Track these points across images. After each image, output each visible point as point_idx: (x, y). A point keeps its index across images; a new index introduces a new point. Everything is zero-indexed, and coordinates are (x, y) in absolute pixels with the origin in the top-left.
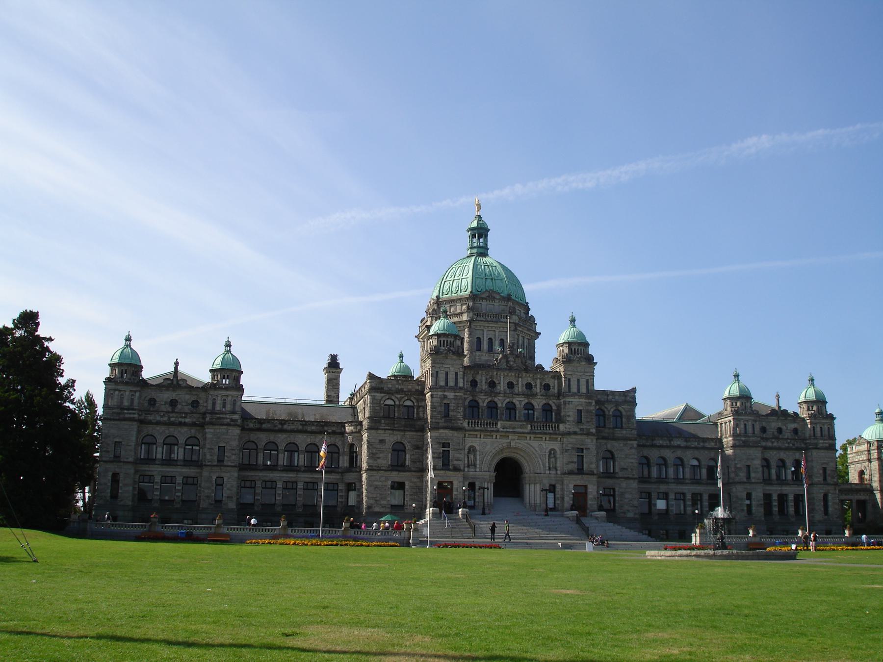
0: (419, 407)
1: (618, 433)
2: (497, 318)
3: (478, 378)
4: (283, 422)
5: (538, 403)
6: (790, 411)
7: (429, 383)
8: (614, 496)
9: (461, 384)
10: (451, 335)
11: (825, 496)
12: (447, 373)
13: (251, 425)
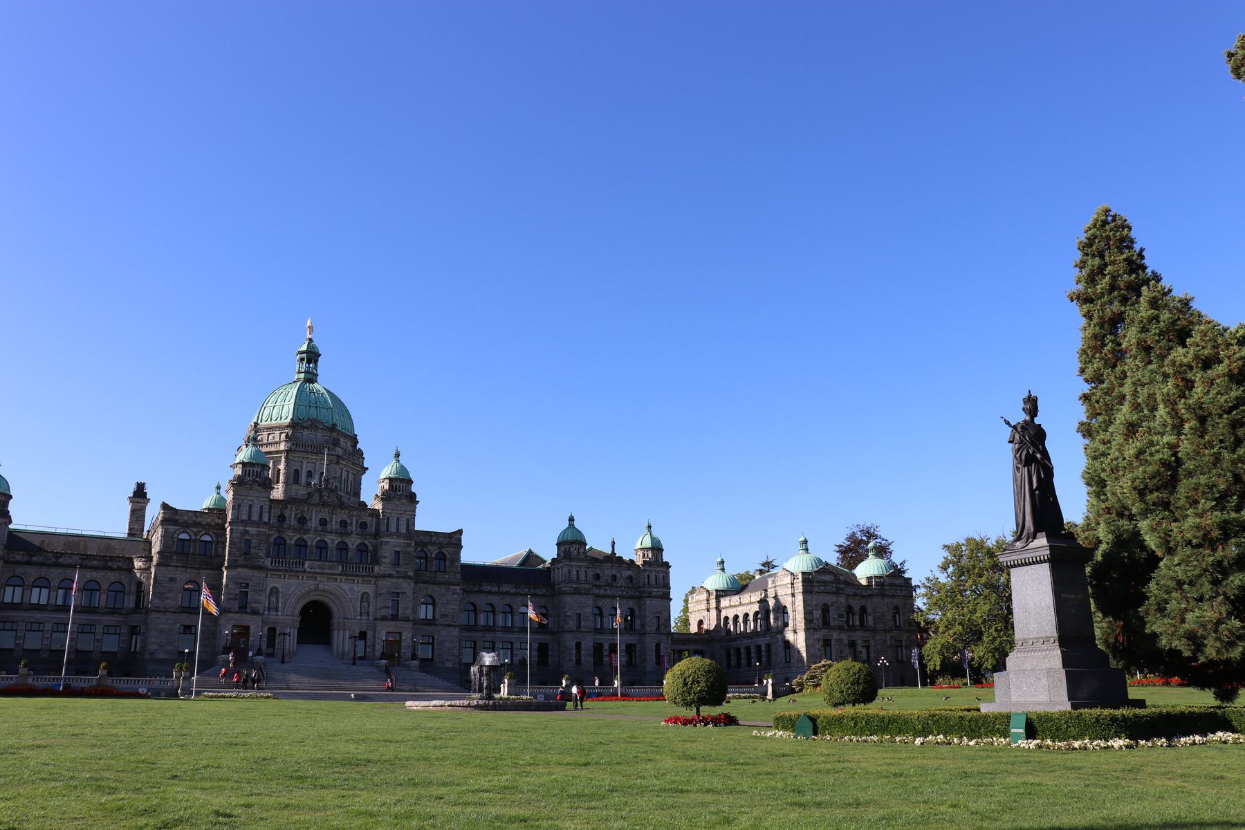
1: (441, 577)
3: (287, 513)
4: (58, 555)
5: (353, 542)
6: (626, 558)
8: (432, 644)
9: (266, 519)
10: (258, 464)
11: (658, 646)
13: (18, 558)
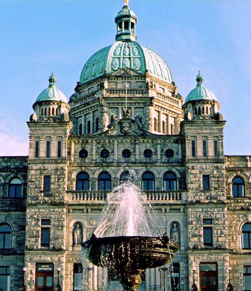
0: (25, 184)
3: (88, 148)
12: (48, 144)
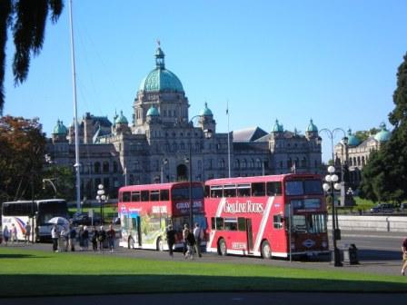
2: (171, 102)
5: (193, 141)
7: (148, 136)
